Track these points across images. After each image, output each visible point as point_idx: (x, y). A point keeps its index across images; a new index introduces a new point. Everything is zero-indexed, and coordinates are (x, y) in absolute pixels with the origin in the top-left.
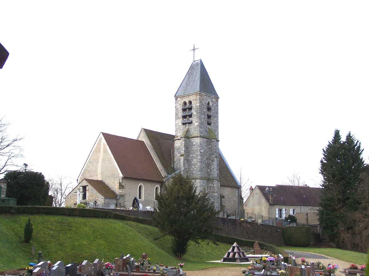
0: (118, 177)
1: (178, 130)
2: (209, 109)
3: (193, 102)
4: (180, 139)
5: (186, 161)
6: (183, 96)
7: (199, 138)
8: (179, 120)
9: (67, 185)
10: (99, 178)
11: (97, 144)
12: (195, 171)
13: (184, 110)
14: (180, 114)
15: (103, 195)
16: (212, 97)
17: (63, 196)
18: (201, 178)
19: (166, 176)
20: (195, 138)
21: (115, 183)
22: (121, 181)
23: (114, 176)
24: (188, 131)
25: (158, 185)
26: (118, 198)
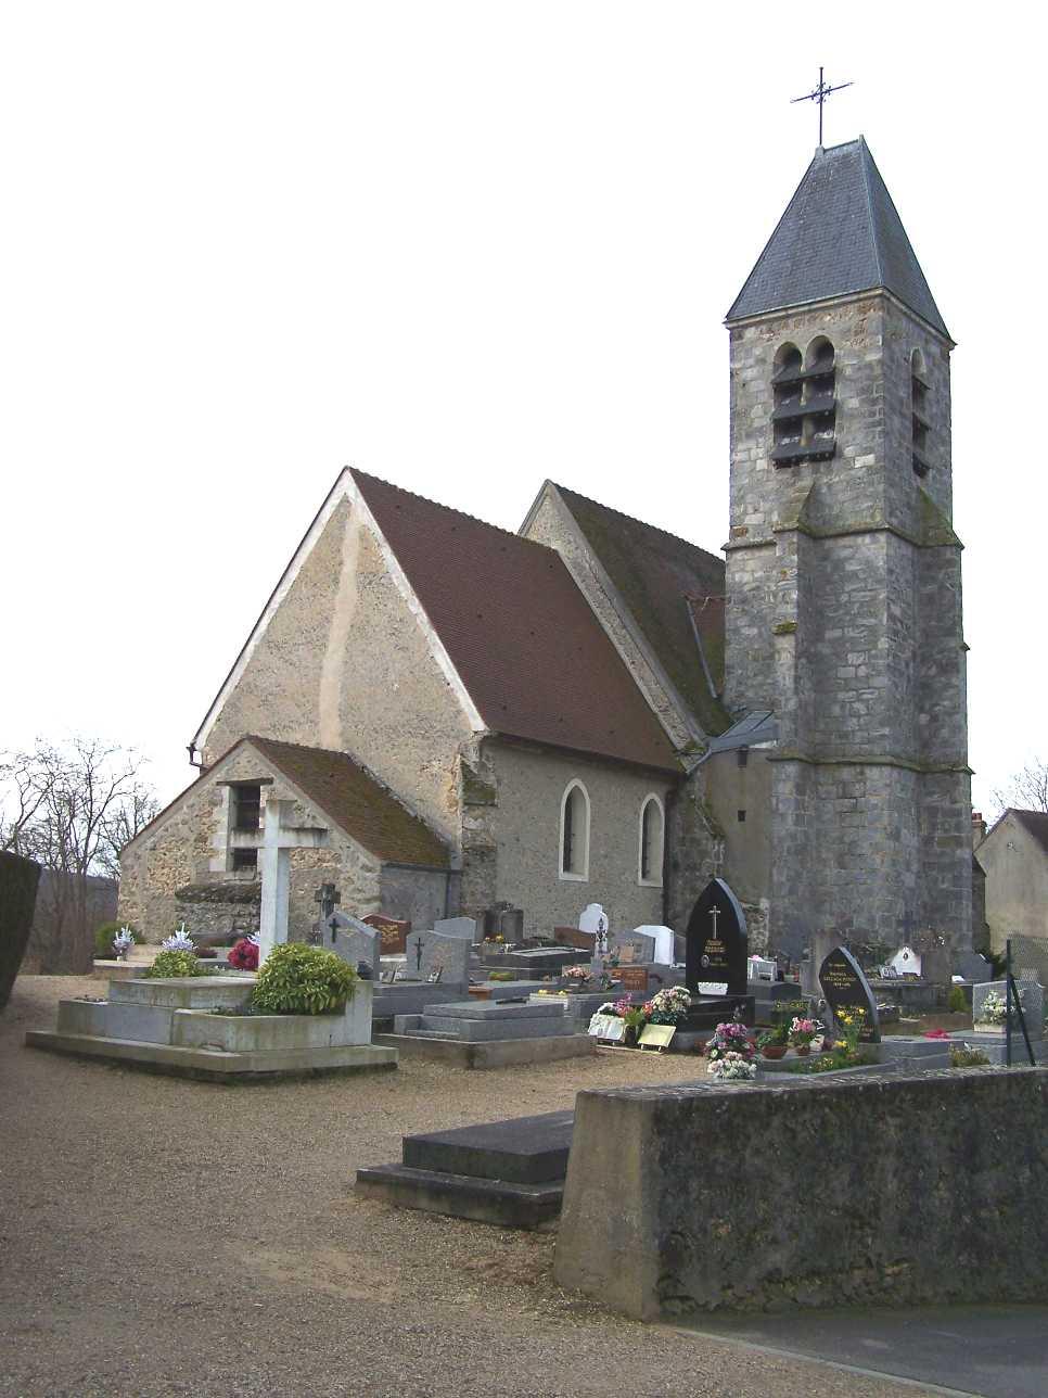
0: (457, 738)
1: (749, 498)
2: (918, 389)
3: (841, 348)
4: (772, 544)
5: (803, 661)
6: (783, 313)
7: (882, 538)
8: (751, 444)
9: (116, 779)
10: (329, 737)
11: (329, 532)
12: (855, 720)
13: (785, 389)
14: (757, 410)
15: (371, 845)
16: (930, 333)
17: (96, 828)
18: (895, 761)
19: (693, 744)
20: (859, 540)
21: (436, 767)
22: (473, 757)
23: (428, 727)
24: (813, 499)
25: (657, 793)
26: (455, 866)
